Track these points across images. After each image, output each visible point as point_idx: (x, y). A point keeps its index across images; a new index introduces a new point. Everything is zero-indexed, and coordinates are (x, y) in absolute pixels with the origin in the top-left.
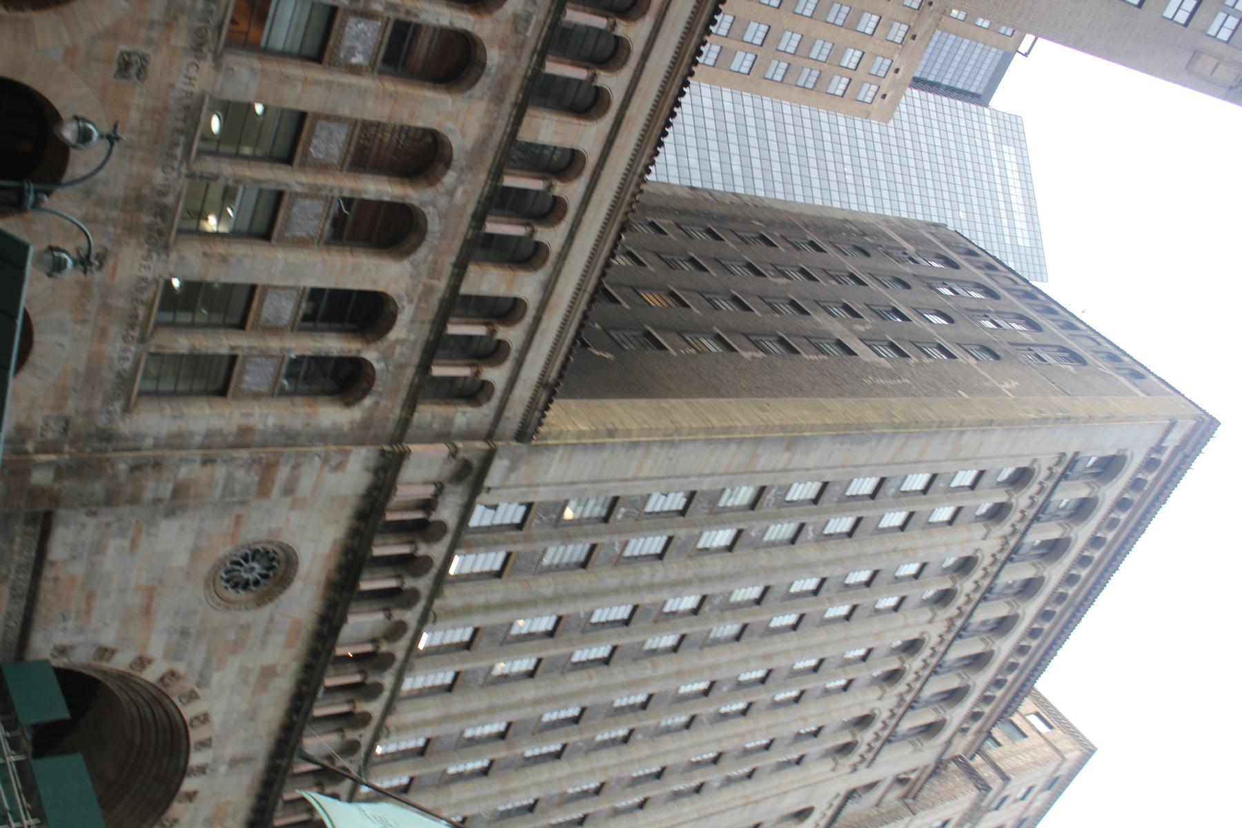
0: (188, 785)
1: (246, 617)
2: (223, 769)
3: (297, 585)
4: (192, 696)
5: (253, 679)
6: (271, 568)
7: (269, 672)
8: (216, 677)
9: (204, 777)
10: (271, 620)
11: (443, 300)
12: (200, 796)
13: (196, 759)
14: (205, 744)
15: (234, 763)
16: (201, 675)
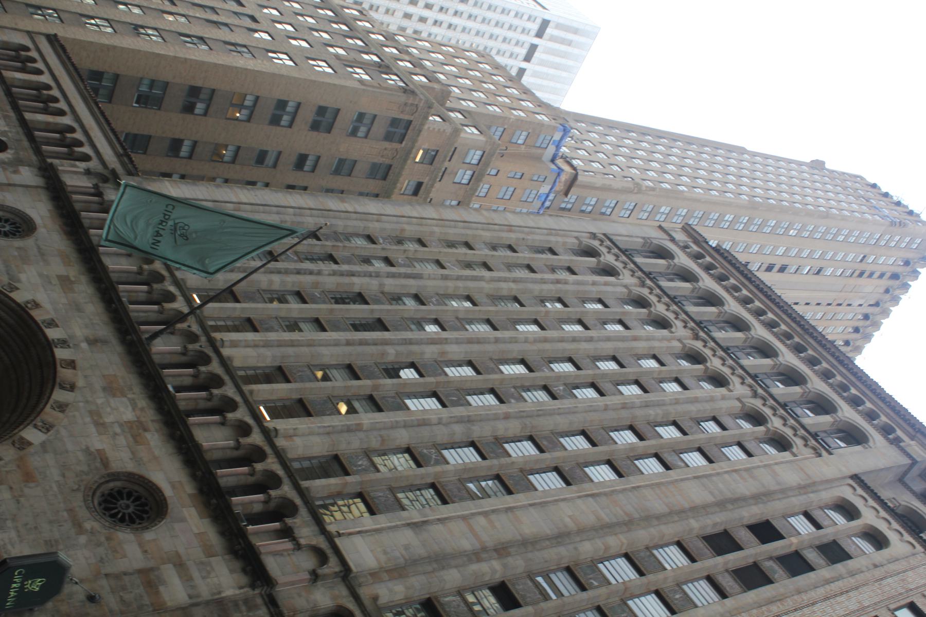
0: (61, 354)
1: (17, 243)
2: (84, 345)
3: (41, 231)
4: (15, 289)
5: (55, 281)
6: (14, 223)
7: (65, 281)
8: (23, 277)
9: (72, 350)
10: (39, 248)
11: (18, 120)
12: (79, 363)
13: (52, 334)
14: (52, 324)
15: (93, 342)
16: (8, 274)
